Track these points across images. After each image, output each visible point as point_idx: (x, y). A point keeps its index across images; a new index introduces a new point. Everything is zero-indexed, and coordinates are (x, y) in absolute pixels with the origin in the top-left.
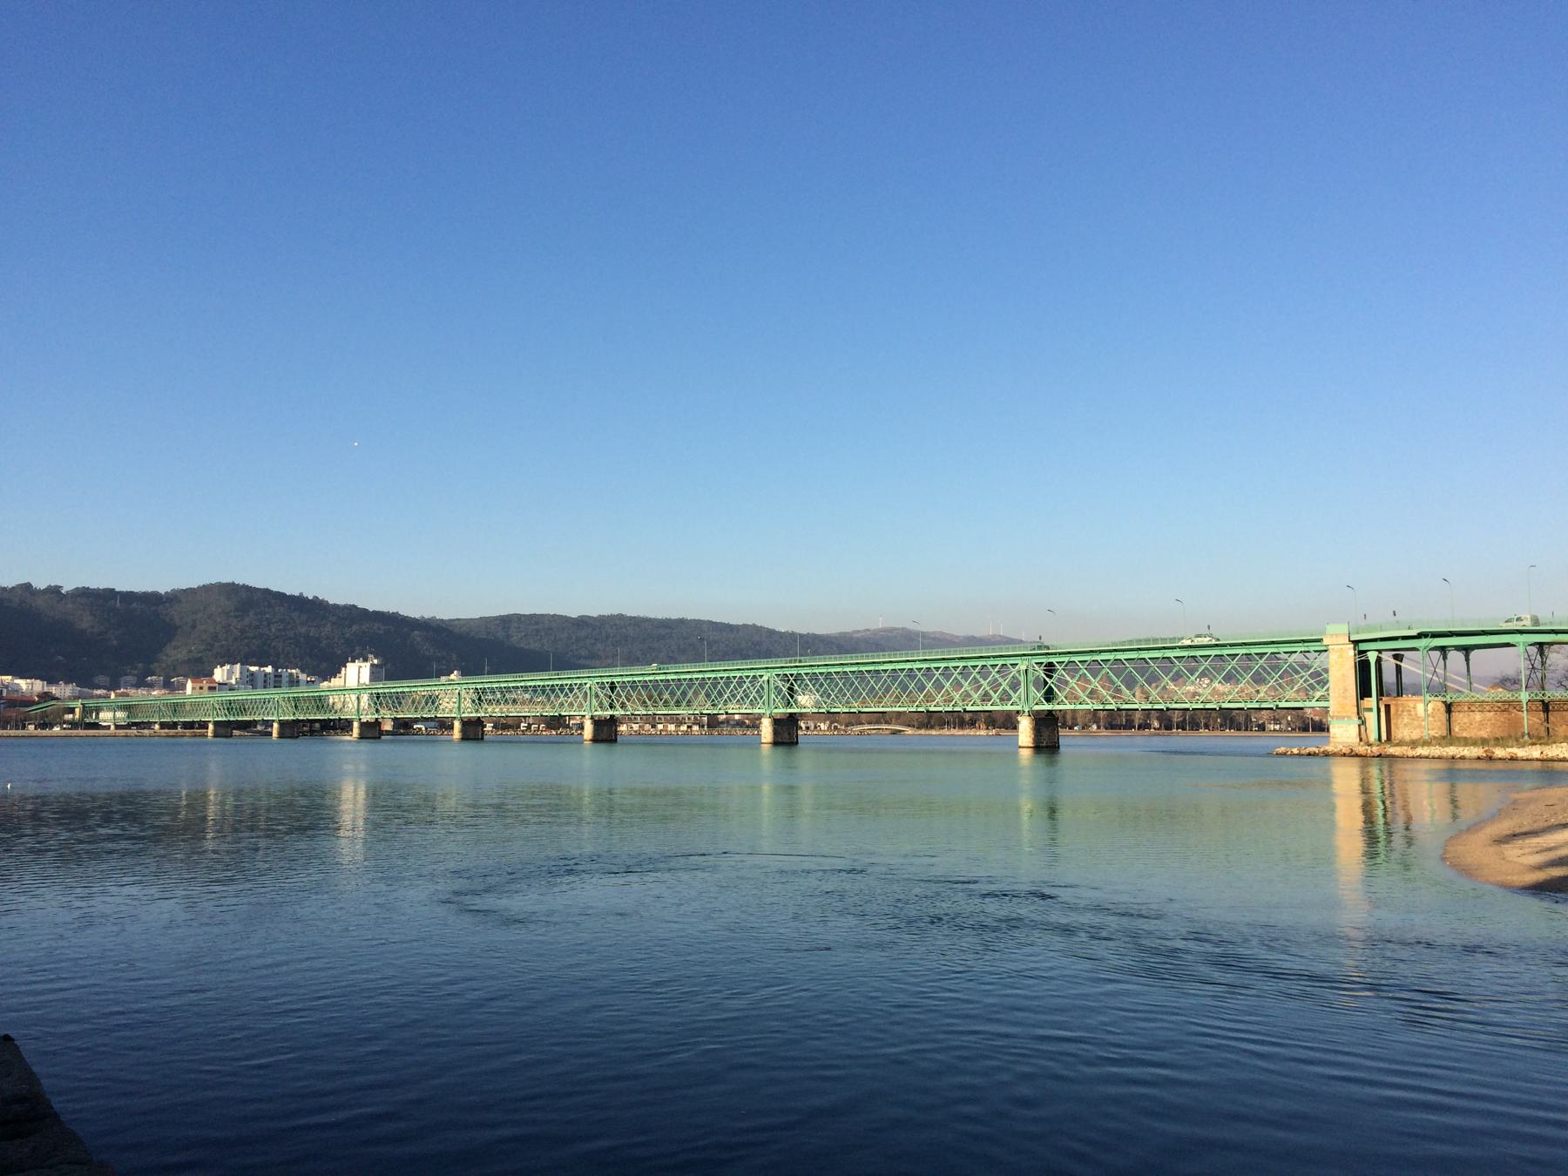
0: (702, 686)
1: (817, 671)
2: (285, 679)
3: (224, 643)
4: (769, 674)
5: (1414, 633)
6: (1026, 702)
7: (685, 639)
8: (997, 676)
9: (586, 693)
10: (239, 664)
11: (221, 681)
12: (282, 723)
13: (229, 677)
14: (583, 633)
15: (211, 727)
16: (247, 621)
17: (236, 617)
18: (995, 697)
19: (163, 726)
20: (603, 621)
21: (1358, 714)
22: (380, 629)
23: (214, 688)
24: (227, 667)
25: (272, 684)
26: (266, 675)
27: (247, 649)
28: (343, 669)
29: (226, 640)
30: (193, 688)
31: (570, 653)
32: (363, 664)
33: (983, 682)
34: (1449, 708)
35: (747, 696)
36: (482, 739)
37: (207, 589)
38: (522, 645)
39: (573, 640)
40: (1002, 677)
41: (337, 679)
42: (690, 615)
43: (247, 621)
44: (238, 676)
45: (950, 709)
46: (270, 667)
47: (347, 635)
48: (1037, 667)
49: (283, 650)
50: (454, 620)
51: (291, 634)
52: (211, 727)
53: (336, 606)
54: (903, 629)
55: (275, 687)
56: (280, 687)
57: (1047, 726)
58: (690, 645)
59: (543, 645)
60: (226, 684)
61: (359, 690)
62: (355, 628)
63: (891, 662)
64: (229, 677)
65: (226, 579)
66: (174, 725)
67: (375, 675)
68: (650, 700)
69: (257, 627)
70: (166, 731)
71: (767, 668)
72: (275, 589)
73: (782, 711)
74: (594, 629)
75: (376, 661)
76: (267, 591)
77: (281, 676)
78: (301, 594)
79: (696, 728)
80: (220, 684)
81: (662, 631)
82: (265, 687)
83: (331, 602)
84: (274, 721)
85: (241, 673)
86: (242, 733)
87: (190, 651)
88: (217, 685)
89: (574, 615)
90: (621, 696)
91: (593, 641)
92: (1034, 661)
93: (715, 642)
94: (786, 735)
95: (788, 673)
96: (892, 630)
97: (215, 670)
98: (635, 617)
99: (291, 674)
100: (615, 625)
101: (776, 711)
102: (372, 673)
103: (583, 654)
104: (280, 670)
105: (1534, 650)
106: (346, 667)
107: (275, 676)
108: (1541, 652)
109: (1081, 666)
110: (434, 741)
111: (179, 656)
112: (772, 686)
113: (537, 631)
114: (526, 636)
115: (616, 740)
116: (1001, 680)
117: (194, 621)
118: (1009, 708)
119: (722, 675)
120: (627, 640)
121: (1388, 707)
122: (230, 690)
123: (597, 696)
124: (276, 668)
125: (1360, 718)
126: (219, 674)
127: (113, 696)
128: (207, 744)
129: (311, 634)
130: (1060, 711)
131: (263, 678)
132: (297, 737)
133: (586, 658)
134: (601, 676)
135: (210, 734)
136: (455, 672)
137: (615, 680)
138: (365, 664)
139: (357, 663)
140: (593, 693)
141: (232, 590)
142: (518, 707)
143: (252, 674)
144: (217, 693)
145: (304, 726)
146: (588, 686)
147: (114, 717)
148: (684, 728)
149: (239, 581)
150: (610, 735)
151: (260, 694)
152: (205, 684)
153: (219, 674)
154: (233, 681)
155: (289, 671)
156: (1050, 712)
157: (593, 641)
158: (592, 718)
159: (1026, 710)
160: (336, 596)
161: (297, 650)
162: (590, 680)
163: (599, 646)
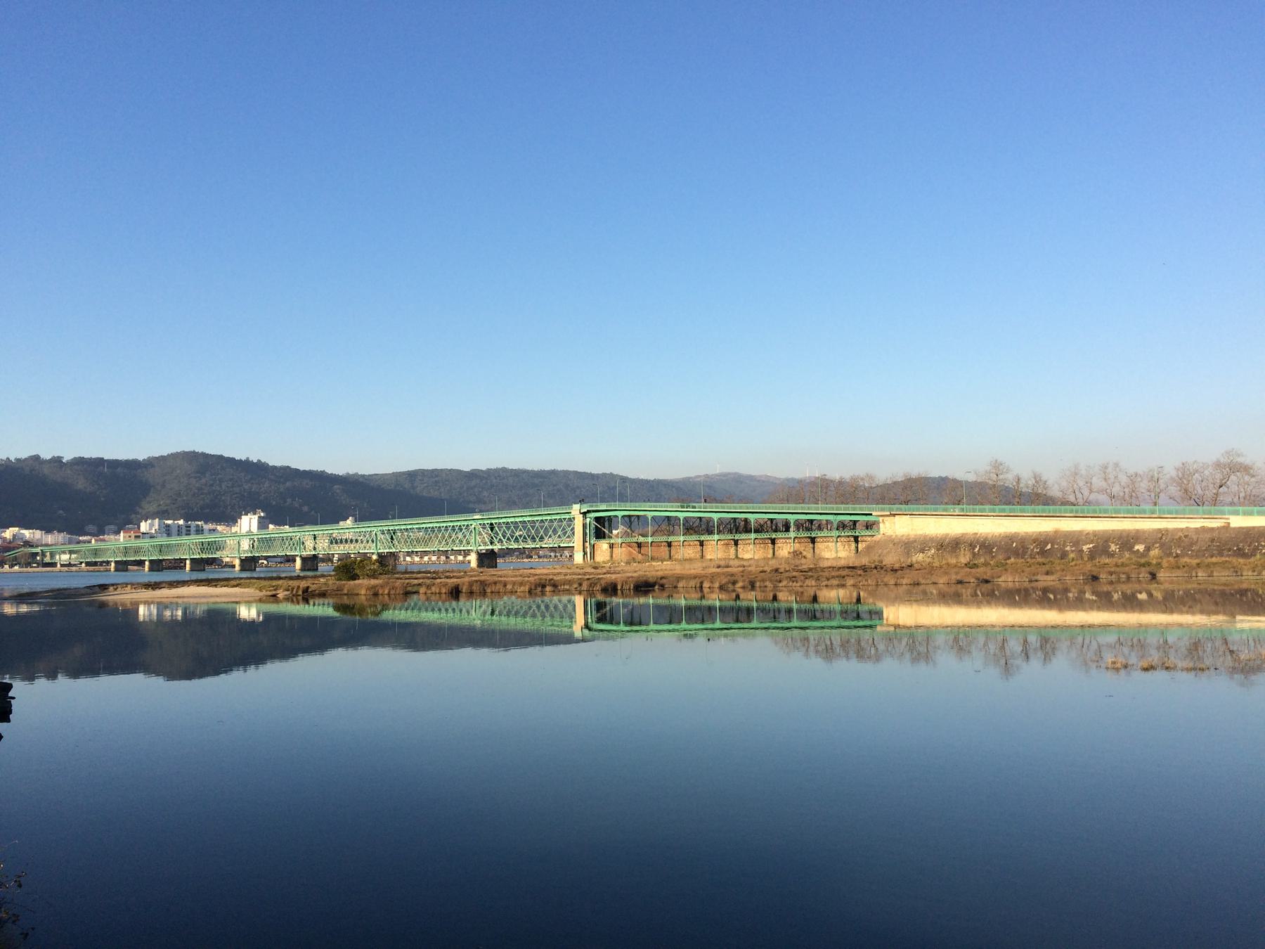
2: (193, 529)
3: (185, 498)
7: (554, 486)
9: (471, 531)
10: (157, 520)
11: (145, 532)
12: (151, 561)
13: (151, 529)
14: (473, 483)
16: (203, 481)
17: (195, 478)
19: (88, 564)
22: (307, 484)
24: (149, 521)
27: (202, 502)
29: (186, 496)
30: (124, 537)
32: (253, 517)
34: (611, 546)
37: (174, 456)
38: (424, 494)
39: (465, 488)
41: (236, 527)
42: (560, 467)
43: (203, 481)
44: (157, 527)
46: (182, 520)
47: (282, 490)
50: (373, 475)
51: (237, 490)
52: (113, 564)
53: (275, 467)
54: (736, 473)
55: (186, 535)
56: (189, 534)
59: (440, 493)
61: (250, 533)
62: (288, 484)
64: (151, 529)
66: (95, 564)
67: (262, 525)
68: (504, 538)
69: (212, 485)
70: (88, 567)
72: (226, 455)
73: (483, 548)
74: (481, 480)
75: (262, 514)
76: (221, 457)
77: (190, 527)
78: (248, 458)
80: (143, 533)
81: (536, 481)
82: (178, 535)
84: (145, 560)
85: (159, 525)
87: (160, 505)
88: (141, 534)
89: (467, 468)
90: (498, 535)
93: (578, 487)
96: (726, 475)
99: (198, 526)
103: (471, 500)
104: (189, 523)
105: (626, 519)
108: (638, 519)
120: (507, 488)
121: (594, 545)
122: (151, 538)
123: (480, 534)
124: (186, 521)
125: (584, 551)
126: (144, 527)
127: (93, 541)
129: (253, 490)
131: (177, 529)
132: (162, 570)
133: (474, 503)
135: (112, 569)
136: (350, 518)
137: (493, 521)
139: (250, 516)
141: (192, 456)
142: (357, 545)
143: (168, 526)
144: (142, 541)
146: (473, 526)
147: (70, 558)
149: (199, 449)
150: (313, 566)
151: (174, 540)
152: (132, 534)
153: (144, 527)
154: (153, 531)
155: (197, 523)
158: (301, 556)
160: (275, 459)
161: (241, 502)
162: (476, 520)
163: (485, 494)
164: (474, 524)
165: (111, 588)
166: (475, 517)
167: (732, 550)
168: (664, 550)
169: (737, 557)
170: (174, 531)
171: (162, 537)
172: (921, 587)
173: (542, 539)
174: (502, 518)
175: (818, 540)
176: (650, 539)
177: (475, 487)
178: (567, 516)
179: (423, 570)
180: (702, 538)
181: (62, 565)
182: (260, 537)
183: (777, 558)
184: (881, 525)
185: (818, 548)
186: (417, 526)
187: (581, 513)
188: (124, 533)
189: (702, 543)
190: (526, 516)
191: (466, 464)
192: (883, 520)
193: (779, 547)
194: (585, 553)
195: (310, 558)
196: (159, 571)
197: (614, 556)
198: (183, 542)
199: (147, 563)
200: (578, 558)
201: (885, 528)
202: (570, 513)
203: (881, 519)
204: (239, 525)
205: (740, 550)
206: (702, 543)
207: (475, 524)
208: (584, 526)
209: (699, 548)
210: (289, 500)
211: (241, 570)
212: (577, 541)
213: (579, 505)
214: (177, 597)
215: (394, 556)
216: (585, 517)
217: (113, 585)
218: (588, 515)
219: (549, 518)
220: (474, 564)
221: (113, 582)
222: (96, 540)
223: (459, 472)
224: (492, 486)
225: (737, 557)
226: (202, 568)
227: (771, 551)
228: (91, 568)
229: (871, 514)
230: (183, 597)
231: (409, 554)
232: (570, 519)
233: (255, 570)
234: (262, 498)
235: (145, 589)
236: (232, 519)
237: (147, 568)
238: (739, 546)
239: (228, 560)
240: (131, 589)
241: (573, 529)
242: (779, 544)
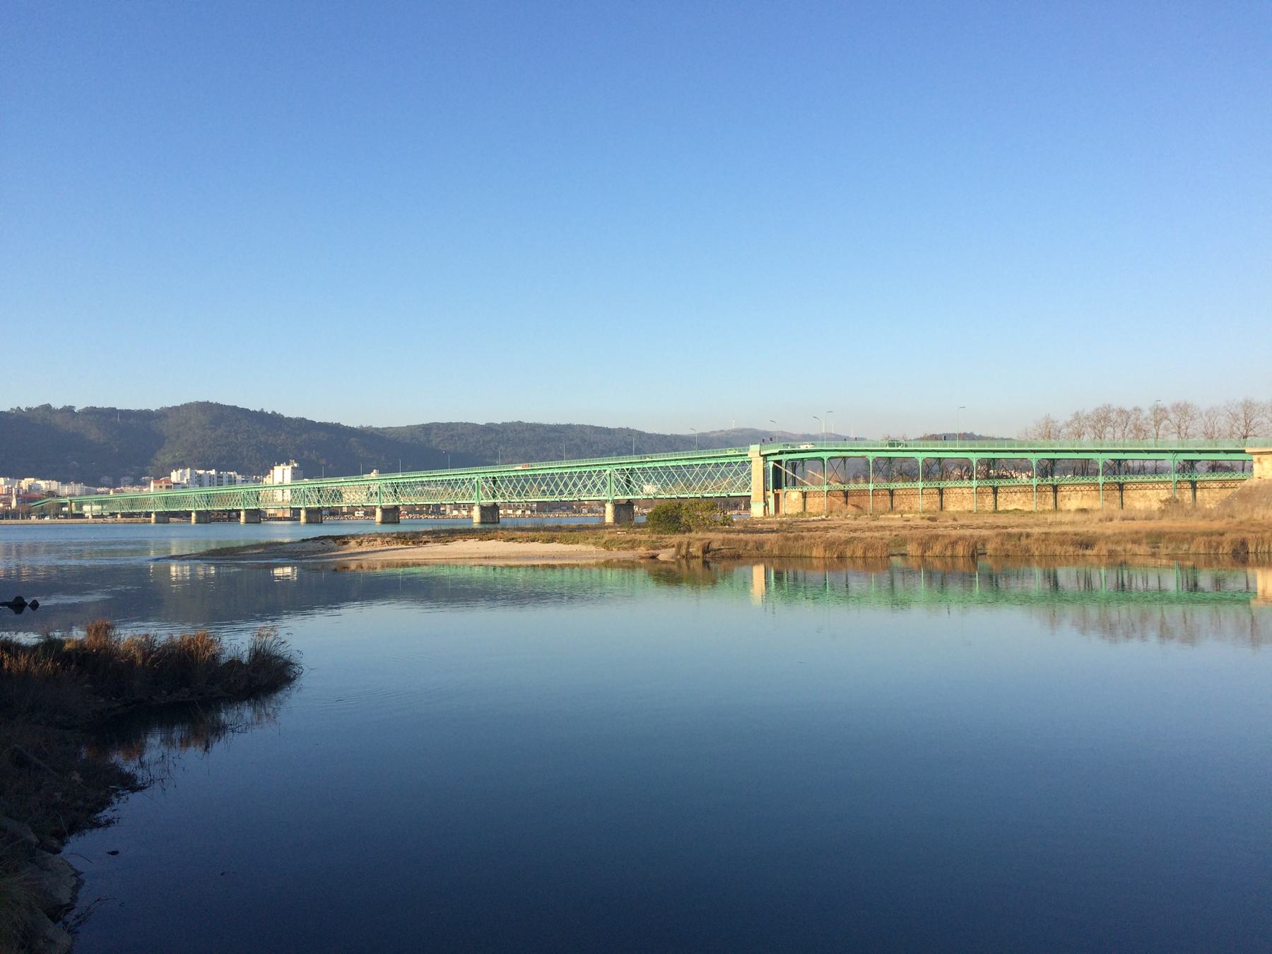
0: (543, 480)
1: (504, 475)
2: (225, 479)
3: (201, 450)
5: (777, 451)
10: (188, 470)
12: (198, 513)
13: (182, 479)
15: (153, 515)
17: (210, 429)
18: (566, 493)
19: (123, 515)
20: (505, 426)
21: (764, 499)
23: (171, 487)
25: (216, 483)
26: (211, 476)
28: (271, 471)
30: (155, 487)
31: (478, 454)
32: (286, 467)
34: (805, 495)
35: (595, 486)
36: (322, 522)
38: (440, 448)
39: (481, 442)
42: (576, 421)
44: (188, 477)
46: (214, 470)
47: (298, 442)
49: (247, 454)
51: (253, 442)
52: (153, 515)
53: (290, 419)
54: (751, 429)
55: (218, 485)
58: (575, 445)
60: (179, 484)
63: (542, 469)
64: (182, 479)
65: (202, 399)
67: (296, 475)
70: (124, 519)
72: (240, 406)
75: (296, 465)
76: (235, 407)
77: (222, 477)
78: (262, 409)
79: (528, 512)
80: (174, 484)
81: (552, 435)
83: (286, 416)
84: (192, 511)
86: (179, 520)
87: (175, 457)
88: (172, 485)
89: (482, 421)
92: (614, 468)
94: (491, 518)
95: (488, 476)
97: (172, 473)
99: (230, 476)
100: (515, 431)
101: (482, 501)
102: (293, 474)
103: (488, 453)
106: (273, 469)
107: (218, 477)
110: (339, 524)
111: (167, 460)
114: (443, 440)
115: (399, 522)
117: (179, 432)
119: (575, 470)
120: (523, 442)
122: (183, 488)
124: (218, 471)
125: (765, 502)
127: (111, 493)
128: (154, 527)
134: (485, 473)
136: (375, 471)
138: (288, 467)
139: (282, 466)
140: (480, 485)
141: (206, 407)
143: (200, 476)
145: (224, 514)
148: (519, 512)
149: (213, 400)
150: (395, 519)
153: (175, 476)
154: (185, 482)
157: (496, 444)
158: (381, 507)
159: (611, 499)
160: (290, 410)
165: (353, 543)
166: (729, 453)
167: (989, 500)
168: (884, 502)
169: (996, 511)
170: (206, 481)
171: (194, 487)
172: (1101, 548)
174: (647, 462)
175: (1129, 487)
176: (871, 487)
178: (740, 460)
179: (530, 526)
180: (893, 486)
181: (93, 517)
182: (294, 487)
183: (1061, 510)
184: (1256, 466)
185: (1129, 497)
187: (762, 456)
188: (154, 483)
189: (941, 492)
192: (1259, 460)
193: (1065, 496)
194: (766, 504)
195: (391, 509)
196: (205, 523)
197: (808, 507)
198: (235, 491)
199: (193, 514)
200: (757, 510)
201: (1263, 469)
202: (747, 455)
203: (1255, 458)
204: (271, 476)
205: (1001, 500)
206: (941, 492)
208: (765, 471)
209: (937, 498)
210: (306, 452)
211: (307, 523)
212: (756, 489)
213: (759, 446)
214: (485, 558)
215: (495, 507)
216: (766, 461)
217: (353, 537)
218: (769, 458)
219: (713, 461)
220: (609, 518)
222: (114, 492)
223: (475, 426)
224: (509, 440)
225: (996, 511)
226: (258, 521)
227: (1052, 501)
228: (129, 520)
229: (1243, 452)
230: (494, 558)
231: (457, 507)
232: (743, 463)
234: (278, 450)
235: (403, 543)
236: (266, 471)
237: (193, 520)
238: (998, 494)
239: (272, 512)
240: (383, 543)
241: (749, 474)
242: (1064, 492)
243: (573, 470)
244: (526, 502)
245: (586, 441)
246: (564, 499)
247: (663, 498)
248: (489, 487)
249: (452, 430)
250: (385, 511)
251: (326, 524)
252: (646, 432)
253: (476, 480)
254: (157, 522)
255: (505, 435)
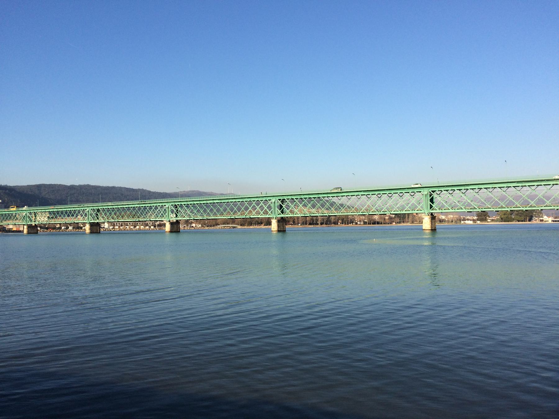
4: (168, 205)
6: (275, 215)
7: (116, 194)
8: (263, 204)
14: (73, 192)
20: (81, 187)
33: (257, 207)
38: (46, 196)
39: (69, 194)
40: (265, 205)
42: (117, 185)
45: (244, 217)
48: (279, 201)
50: (16, 186)
54: (198, 191)
57: (282, 222)
71: (168, 202)
91: (77, 195)
92: (277, 199)
93: (128, 195)
98: (94, 186)
103: (73, 200)
109: (296, 200)
112: (170, 209)
113: (53, 191)
114: (48, 193)
116: (264, 206)
118: (268, 216)
119: (131, 206)
120: (91, 195)
130: (287, 217)
156: (282, 218)
157: (77, 195)
159: (274, 217)
164: (88, 209)
173: (122, 217)
177: (74, 193)
186: (44, 211)
190: (135, 204)
191: (68, 182)
207: (88, 209)
221: (442, 245)
224: (83, 193)
233: (37, 233)
243: (152, 205)
244: (118, 222)
245: (123, 195)
246: (252, 217)
247: (241, 218)
248: (95, 214)
249: (52, 188)
250: (92, 225)
251: (40, 235)
252: (151, 191)
253: (87, 210)
254: (92, 232)
255: (81, 191)
